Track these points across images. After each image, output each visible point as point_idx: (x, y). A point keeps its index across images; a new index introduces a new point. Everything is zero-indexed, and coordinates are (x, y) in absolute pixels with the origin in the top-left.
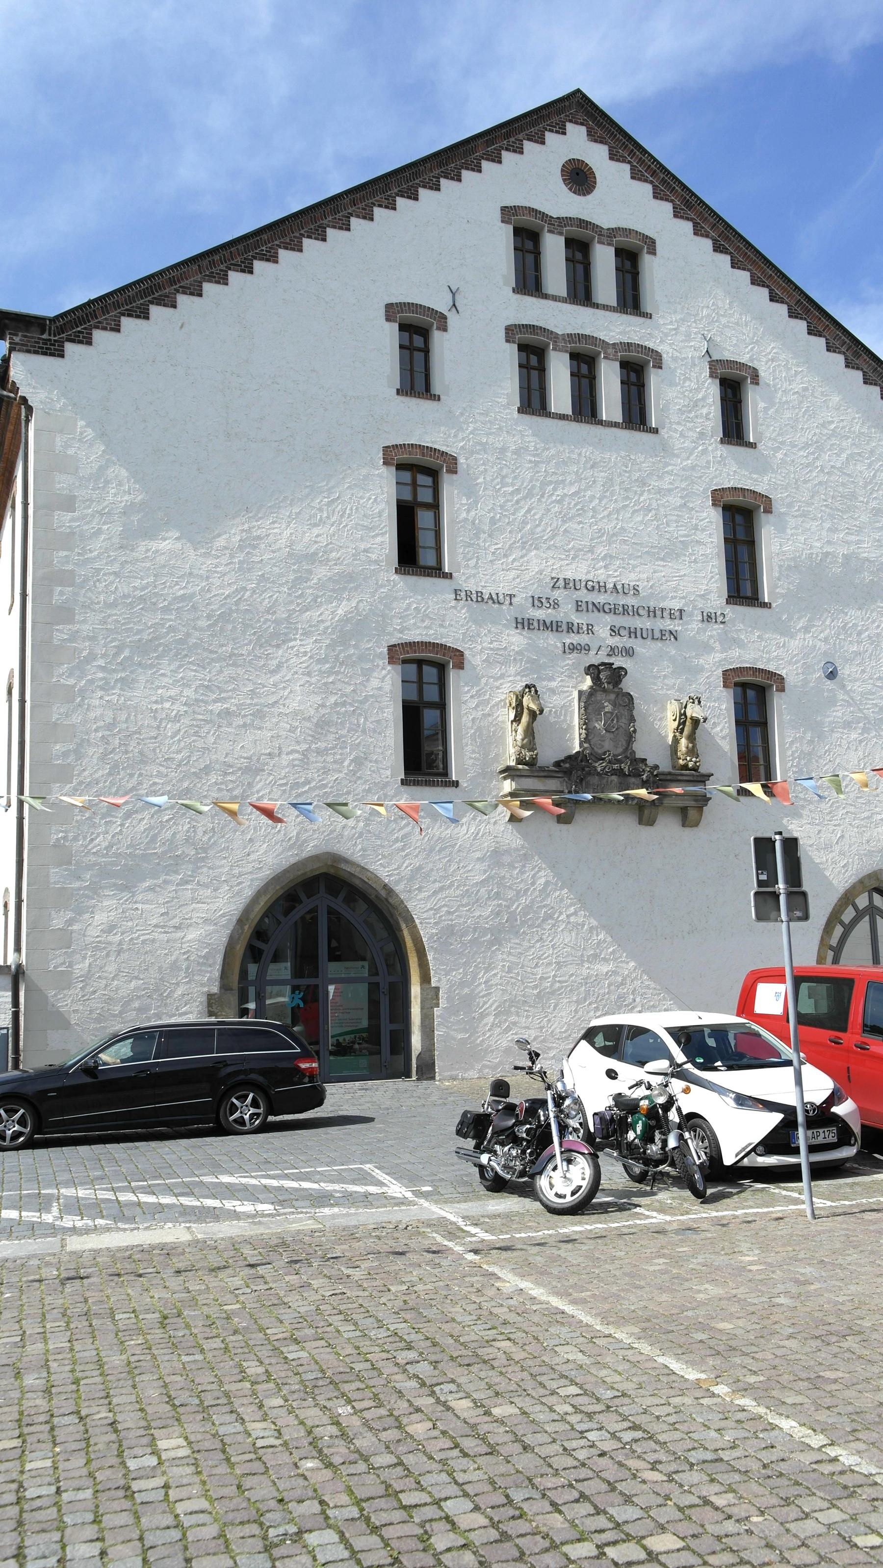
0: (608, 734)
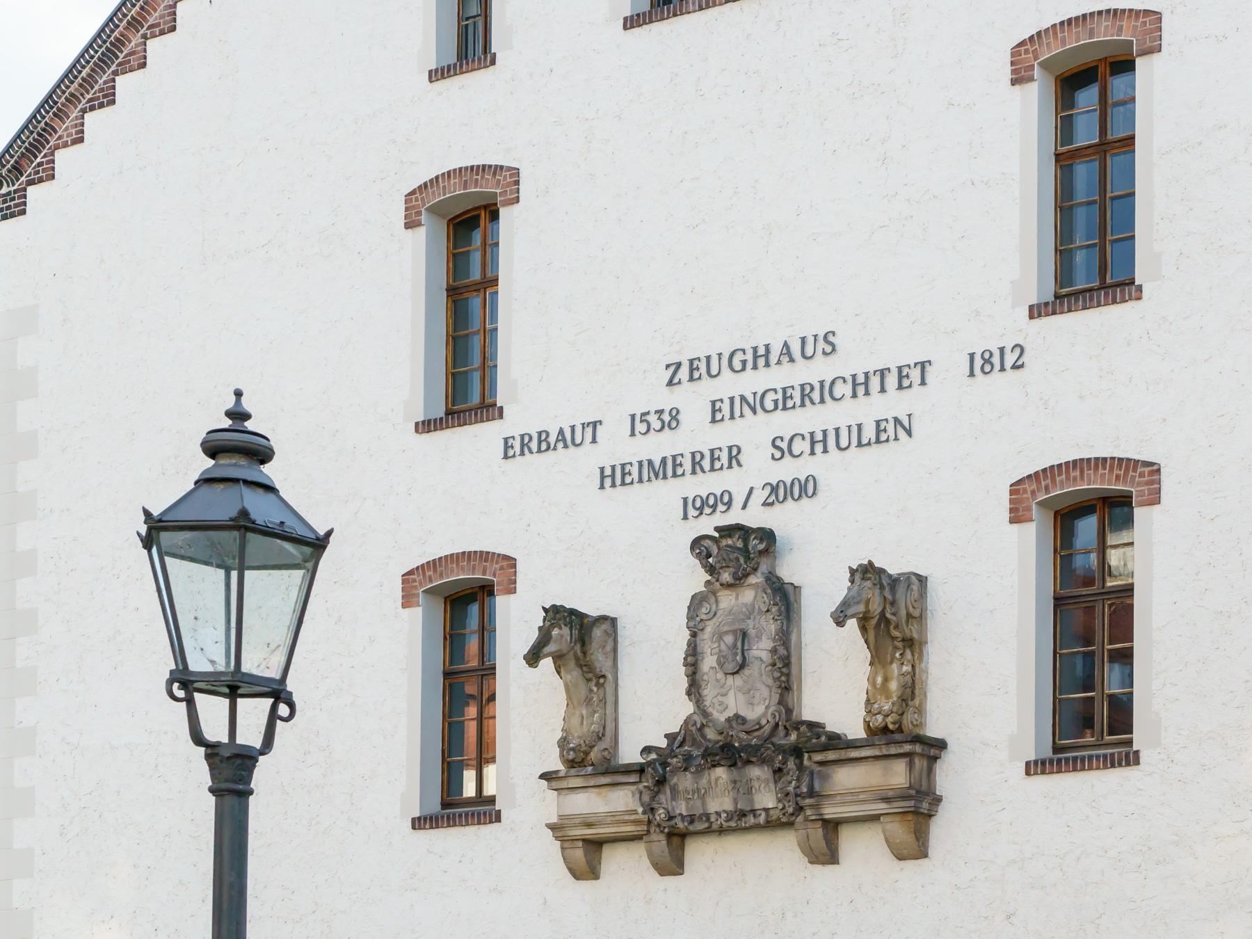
0: (730, 678)
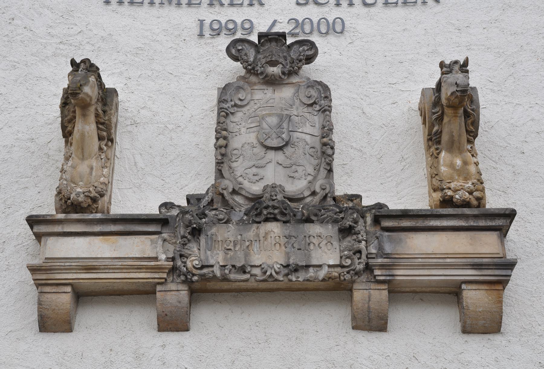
0: (271, 154)
